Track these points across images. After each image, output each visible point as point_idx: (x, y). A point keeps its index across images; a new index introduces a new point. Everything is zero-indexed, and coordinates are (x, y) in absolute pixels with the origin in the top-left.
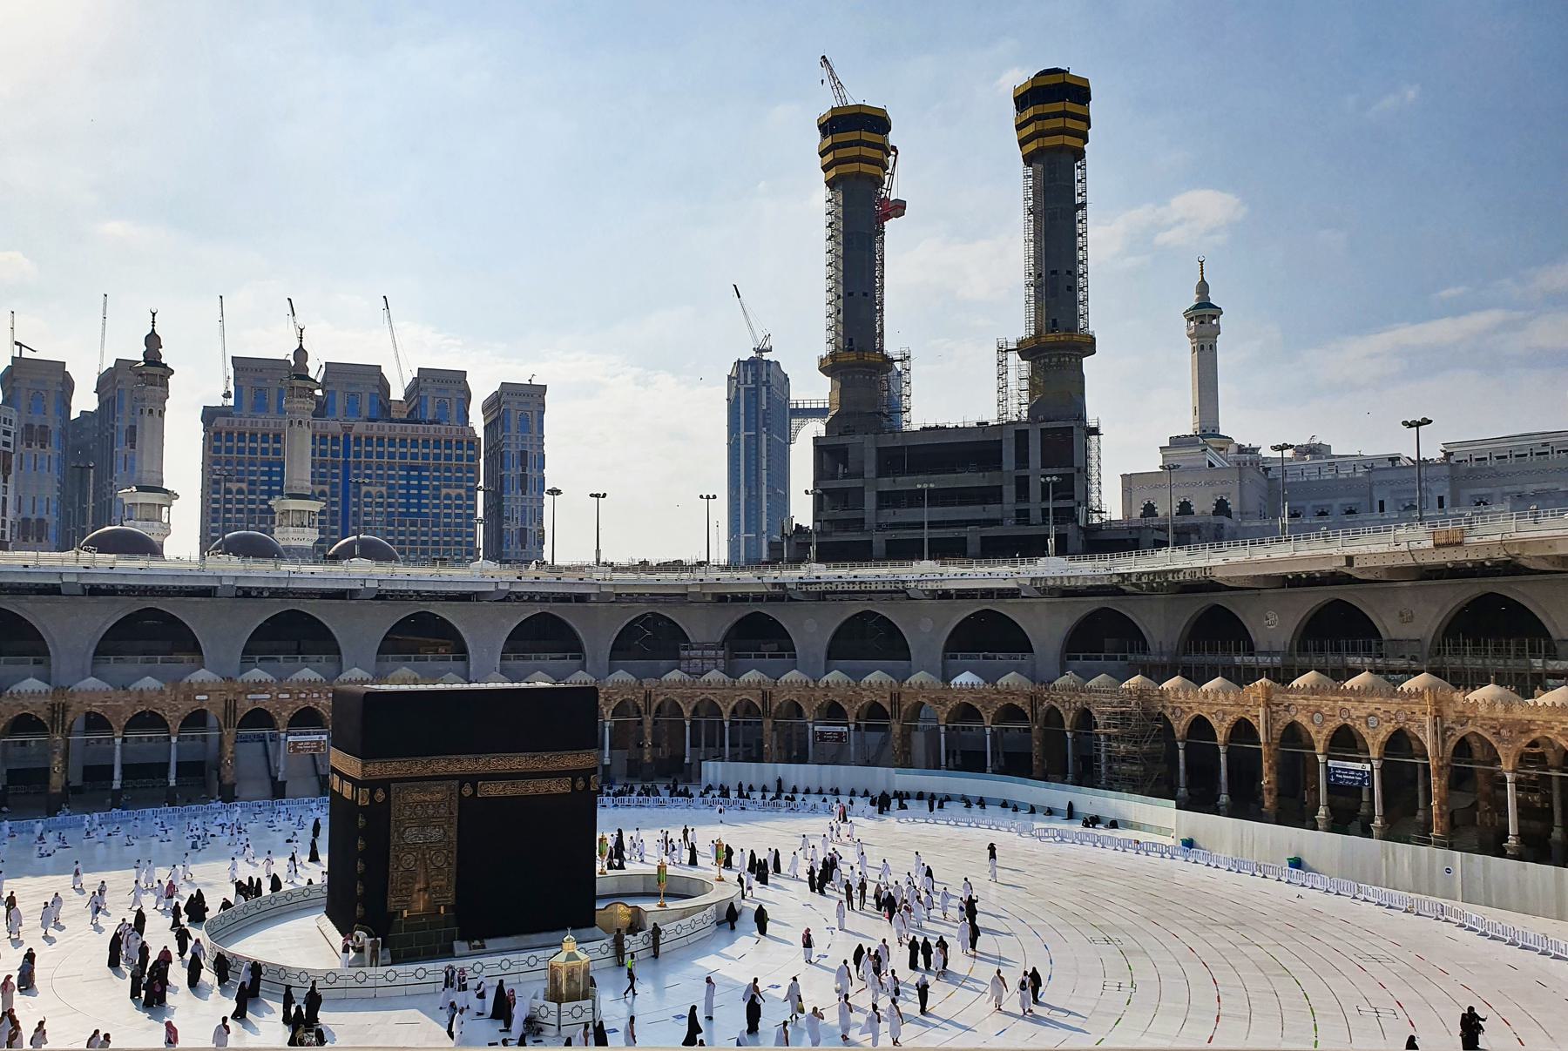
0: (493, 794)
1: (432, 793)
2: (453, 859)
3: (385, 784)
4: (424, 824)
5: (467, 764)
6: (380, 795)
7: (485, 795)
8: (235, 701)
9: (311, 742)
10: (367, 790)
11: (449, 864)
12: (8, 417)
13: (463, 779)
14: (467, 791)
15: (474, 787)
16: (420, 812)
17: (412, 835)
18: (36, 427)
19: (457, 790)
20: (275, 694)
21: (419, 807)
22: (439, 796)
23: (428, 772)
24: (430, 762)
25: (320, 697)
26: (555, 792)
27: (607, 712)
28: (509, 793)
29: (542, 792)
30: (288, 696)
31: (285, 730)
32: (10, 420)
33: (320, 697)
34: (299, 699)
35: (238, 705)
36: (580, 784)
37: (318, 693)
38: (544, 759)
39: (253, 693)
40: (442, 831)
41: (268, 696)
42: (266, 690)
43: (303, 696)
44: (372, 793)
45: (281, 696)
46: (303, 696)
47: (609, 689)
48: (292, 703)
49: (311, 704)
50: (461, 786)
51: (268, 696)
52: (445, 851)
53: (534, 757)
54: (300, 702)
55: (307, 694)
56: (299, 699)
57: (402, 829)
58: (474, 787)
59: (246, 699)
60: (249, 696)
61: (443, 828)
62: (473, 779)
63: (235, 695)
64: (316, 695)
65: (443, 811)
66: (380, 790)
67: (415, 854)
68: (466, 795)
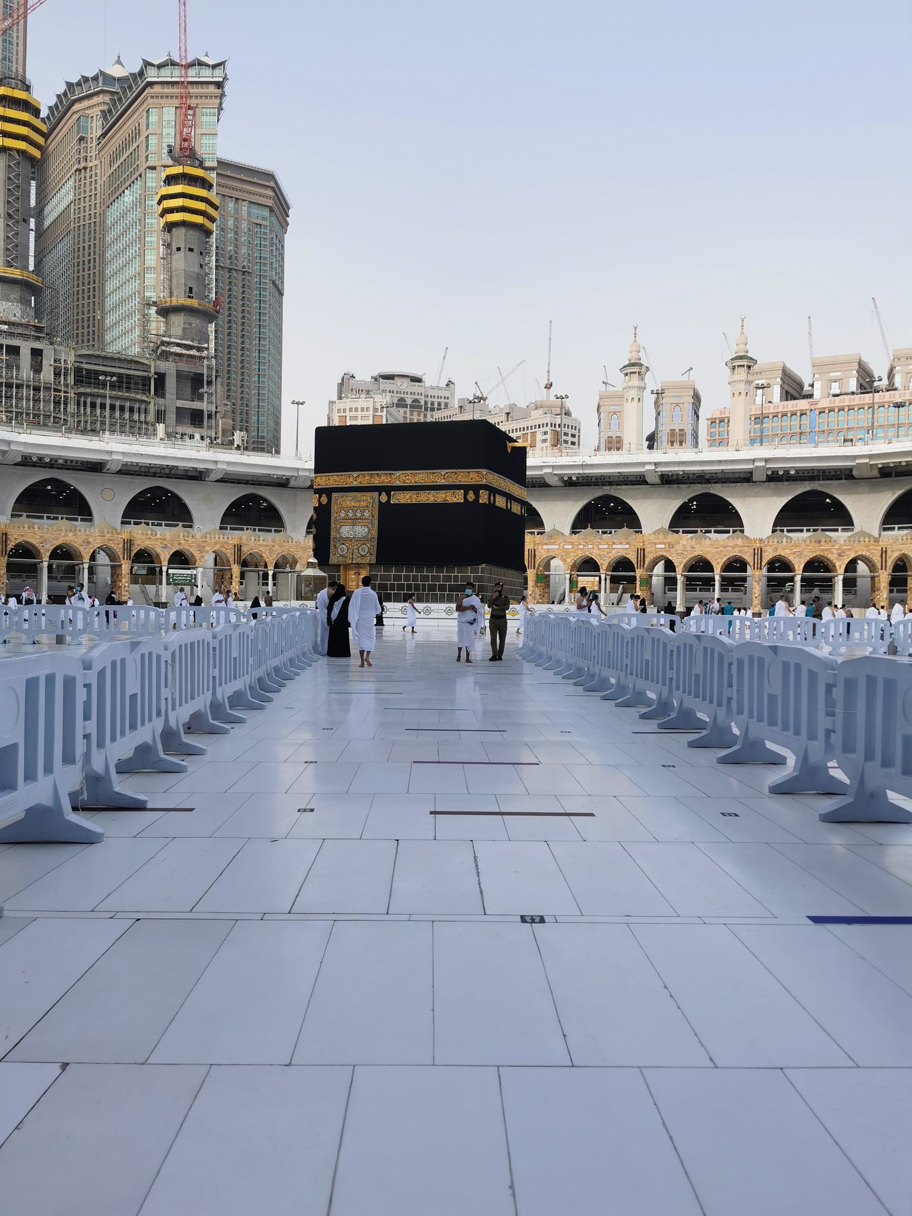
0: (403, 501)
1: (360, 501)
2: (374, 551)
4: (355, 521)
5: (382, 478)
6: (324, 499)
7: (396, 502)
8: (535, 550)
9: (588, 582)
10: (317, 495)
11: (371, 554)
12: (574, 425)
13: (379, 489)
14: (384, 498)
15: (389, 495)
16: (351, 515)
17: (346, 531)
18: (614, 438)
20: (562, 545)
21: (350, 511)
22: (364, 504)
23: (355, 484)
24: (358, 476)
25: (593, 548)
26: (451, 502)
27: (840, 567)
28: (414, 501)
29: (440, 500)
30: (570, 547)
31: (569, 572)
32: (576, 427)
33: (593, 548)
34: (578, 549)
35: (537, 553)
36: (471, 496)
37: (593, 544)
38: (442, 475)
39: (547, 544)
40: (366, 529)
41: (557, 547)
42: (556, 542)
43: (581, 547)
44: (320, 497)
45: (565, 547)
46: (581, 547)
47: (841, 546)
48: (574, 552)
49: (587, 553)
50: (380, 495)
51: (557, 547)
52: (368, 545)
53: (433, 473)
54: (579, 552)
55: (584, 546)
56: (578, 549)
58: (389, 495)
59: (542, 548)
60: (544, 547)
61: (368, 527)
62: (388, 490)
63: (534, 545)
64: (590, 547)
65: (368, 515)
66: (324, 495)
67: (347, 545)
68: (384, 502)
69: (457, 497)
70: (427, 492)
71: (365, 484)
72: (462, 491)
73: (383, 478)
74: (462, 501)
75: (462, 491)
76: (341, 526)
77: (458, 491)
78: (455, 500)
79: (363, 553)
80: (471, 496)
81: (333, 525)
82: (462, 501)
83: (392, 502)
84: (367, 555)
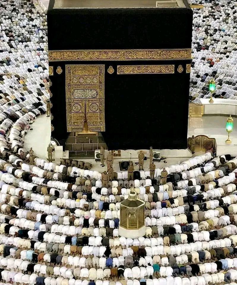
0: (127, 73)
3: (62, 64)
7: (122, 73)
14: (111, 71)
17: (78, 94)
19: (103, 72)
26: (164, 73)
28: (136, 73)
52: (97, 104)
57: (73, 90)
62: (114, 64)
65: (96, 82)
67: (80, 104)
69: (169, 70)
70: (146, 66)
71: (94, 59)
72: (174, 65)
73: (110, 54)
74: (174, 73)
75: (174, 65)
76: (74, 90)
77: (170, 65)
78: (168, 72)
79: (94, 110)
80: (180, 69)
81: (66, 88)
82: (174, 73)
83: (118, 73)
84: (97, 111)
